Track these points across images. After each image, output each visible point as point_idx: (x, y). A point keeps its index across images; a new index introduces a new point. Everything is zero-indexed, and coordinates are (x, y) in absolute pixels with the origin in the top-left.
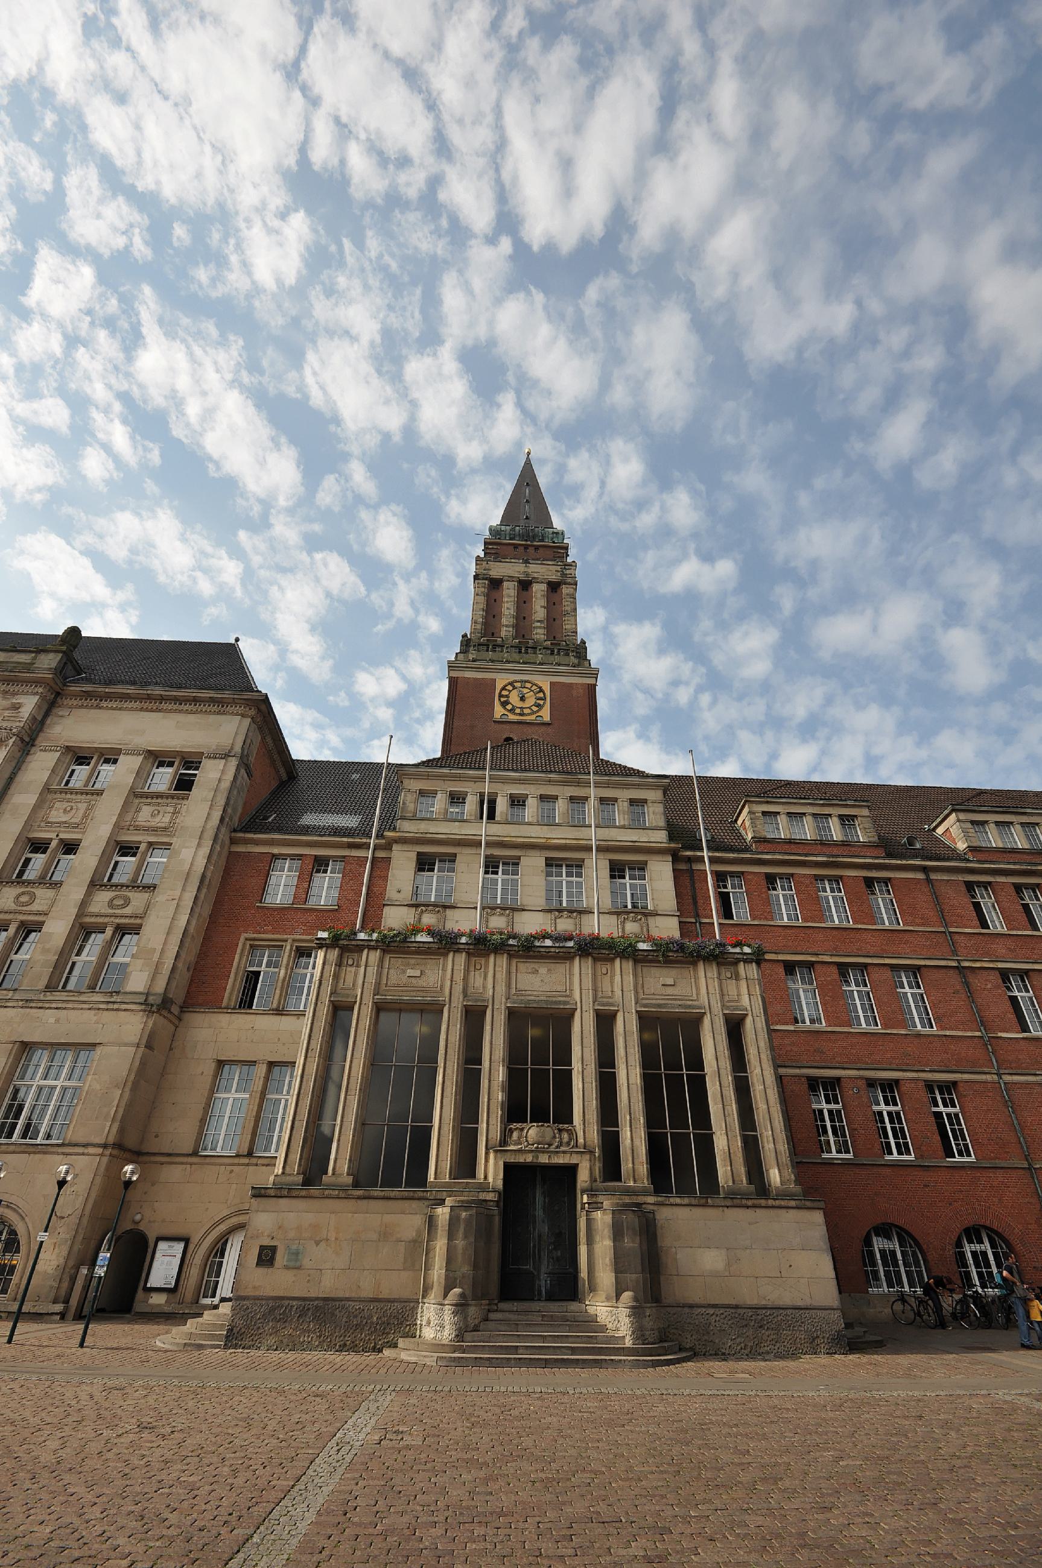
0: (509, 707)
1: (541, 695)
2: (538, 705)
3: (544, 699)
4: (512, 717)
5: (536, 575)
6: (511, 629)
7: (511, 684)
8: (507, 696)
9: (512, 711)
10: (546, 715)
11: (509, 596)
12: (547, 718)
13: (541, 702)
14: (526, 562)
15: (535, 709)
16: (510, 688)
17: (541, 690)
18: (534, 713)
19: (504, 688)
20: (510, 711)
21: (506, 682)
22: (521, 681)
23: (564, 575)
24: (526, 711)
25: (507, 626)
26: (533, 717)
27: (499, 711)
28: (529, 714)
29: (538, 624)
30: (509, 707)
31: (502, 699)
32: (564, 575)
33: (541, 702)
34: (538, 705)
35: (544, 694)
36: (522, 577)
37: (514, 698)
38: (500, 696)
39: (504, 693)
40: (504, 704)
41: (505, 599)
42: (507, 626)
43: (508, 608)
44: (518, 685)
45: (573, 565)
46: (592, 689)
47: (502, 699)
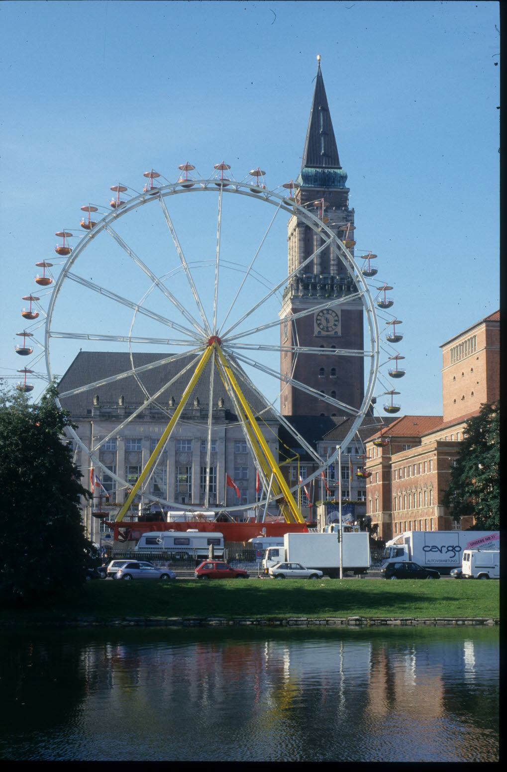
0: (321, 327)
1: (336, 318)
2: (335, 325)
4: (324, 333)
8: (320, 320)
10: (339, 330)
12: (340, 334)
13: (336, 323)
15: (334, 327)
16: (321, 314)
18: (333, 329)
19: (318, 315)
20: (322, 329)
24: (330, 329)
26: (332, 333)
27: (316, 329)
28: (331, 331)
31: (318, 322)
33: (336, 323)
34: (335, 325)
35: (338, 317)
37: (324, 322)
38: (317, 320)
39: (319, 318)
40: (319, 325)
44: (325, 312)
47: (318, 322)
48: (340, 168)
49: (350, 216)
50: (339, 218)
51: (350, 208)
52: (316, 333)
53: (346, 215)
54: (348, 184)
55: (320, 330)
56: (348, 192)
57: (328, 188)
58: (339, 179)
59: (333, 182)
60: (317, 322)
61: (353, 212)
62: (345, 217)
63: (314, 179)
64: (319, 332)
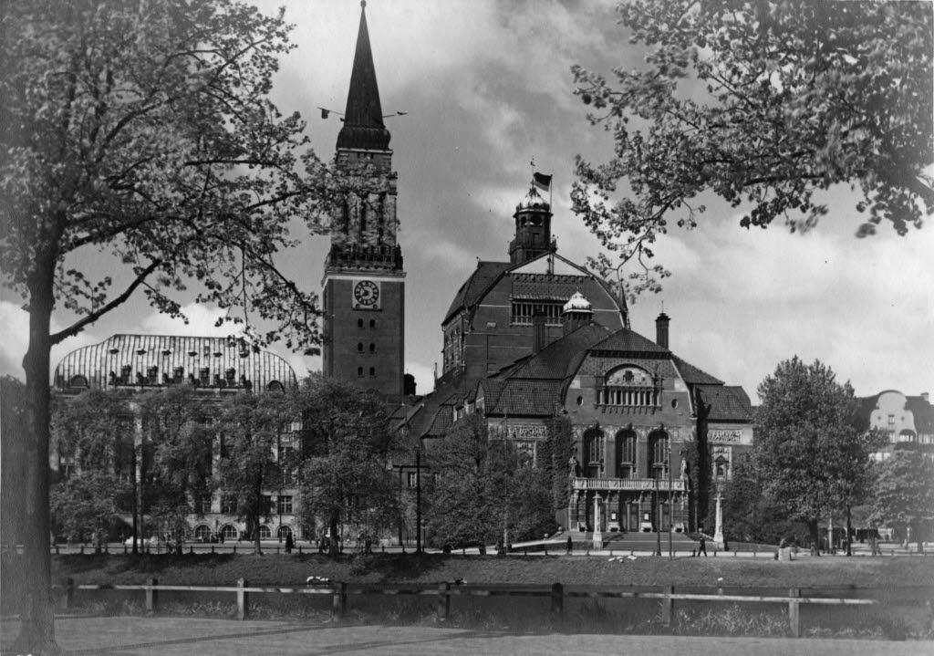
1: (376, 291)
3: (377, 293)
4: (362, 306)
7: (361, 283)
9: (362, 302)
10: (379, 303)
15: (373, 300)
17: (376, 288)
19: (357, 287)
21: (356, 284)
22: (367, 282)
24: (369, 302)
26: (371, 307)
27: (355, 302)
38: (355, 292)
39: (358, 290)
40: (358, 298)
46: (402, 285)
56: (391, 155)
64: (357, 305)
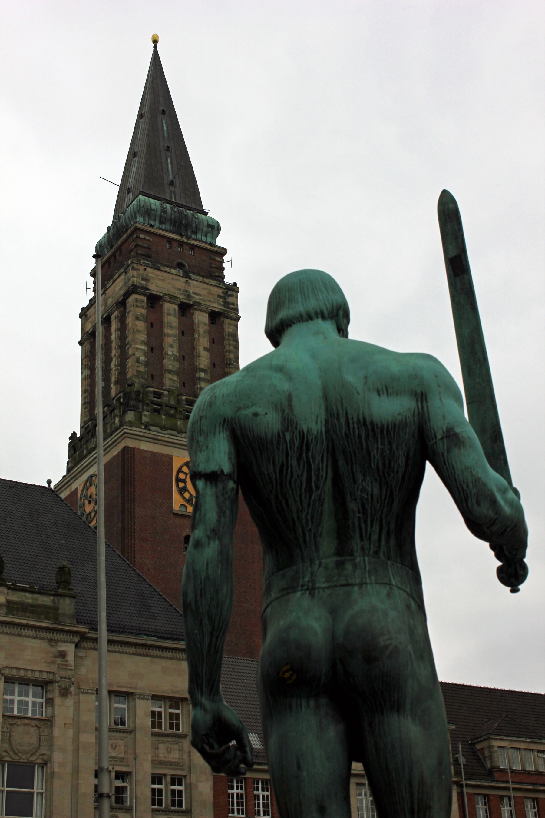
0: (187, 495)
5: (197, 298)
6: (175, 378)
8: (184, 481)
11: (172, 327)
14: (187, 276)
19: (180, 470)
23: (226, 304)
25: (170, 372)
29: (202, 375)
30: (187, 495)
31: (181, 485)
32: (226, 304)
36: (182, 298)
38: (178, 480)
39: (182, 476)
40: (182, 491)
41: (167, 331)
42: (170, 372)
43: (171, 346)
45: (234, 288)
47: (181, 485)
48: (206, 214)
49: (231, 295)
50: (212, 294)
51: (228, 280)
52: (176, 507)
53: (223, 293)
54: (220, 242)
55: (182, 501)
57: (188, 238)
58: (205, 229)
59: (195, 233)
60: (177, 485)
61: (234, 288)
62: (222, 295)
63: (161, 217)
